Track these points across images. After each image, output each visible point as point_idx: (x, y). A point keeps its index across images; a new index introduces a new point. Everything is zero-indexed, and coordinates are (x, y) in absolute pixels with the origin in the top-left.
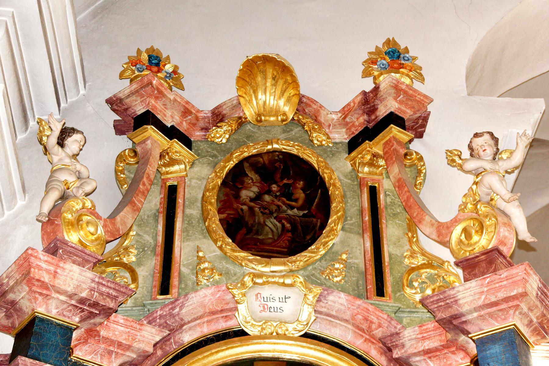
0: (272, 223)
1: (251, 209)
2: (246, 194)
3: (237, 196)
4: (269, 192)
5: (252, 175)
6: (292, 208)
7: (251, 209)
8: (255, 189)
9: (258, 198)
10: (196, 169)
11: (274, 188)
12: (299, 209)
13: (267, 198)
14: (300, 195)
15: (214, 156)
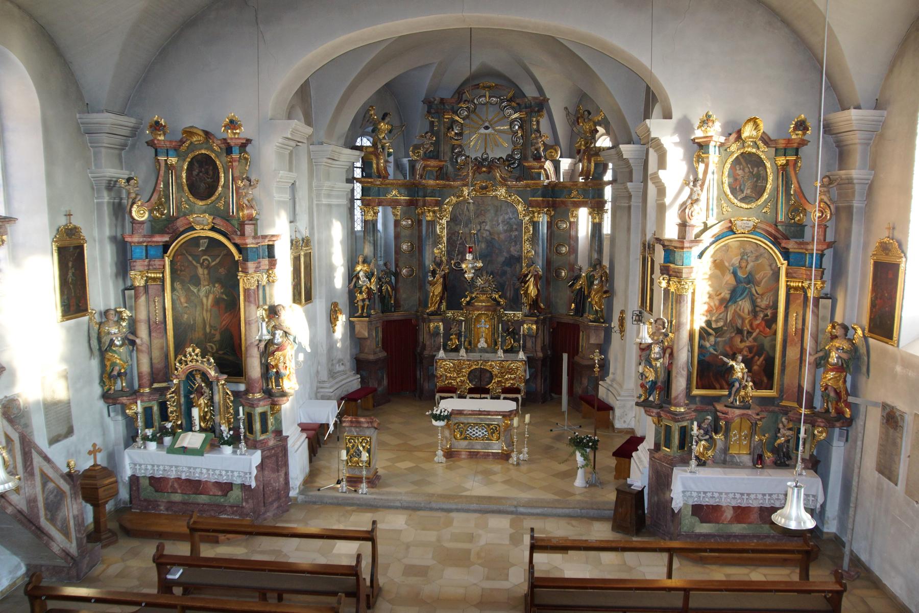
0: (202, 185)
1: (196, 179)
2: (195, 173)
3: (192, 174)
4: (201, 172)
5: (196, 164)
6: (208, 178)
7: (196, 179)
8: (197, 171)
9: (198, 175)
10: (179, 162)
11: (203, 170)
12: (211, 178)
13: (201, 174)
14: (211, 173)
15: (184, 156)
